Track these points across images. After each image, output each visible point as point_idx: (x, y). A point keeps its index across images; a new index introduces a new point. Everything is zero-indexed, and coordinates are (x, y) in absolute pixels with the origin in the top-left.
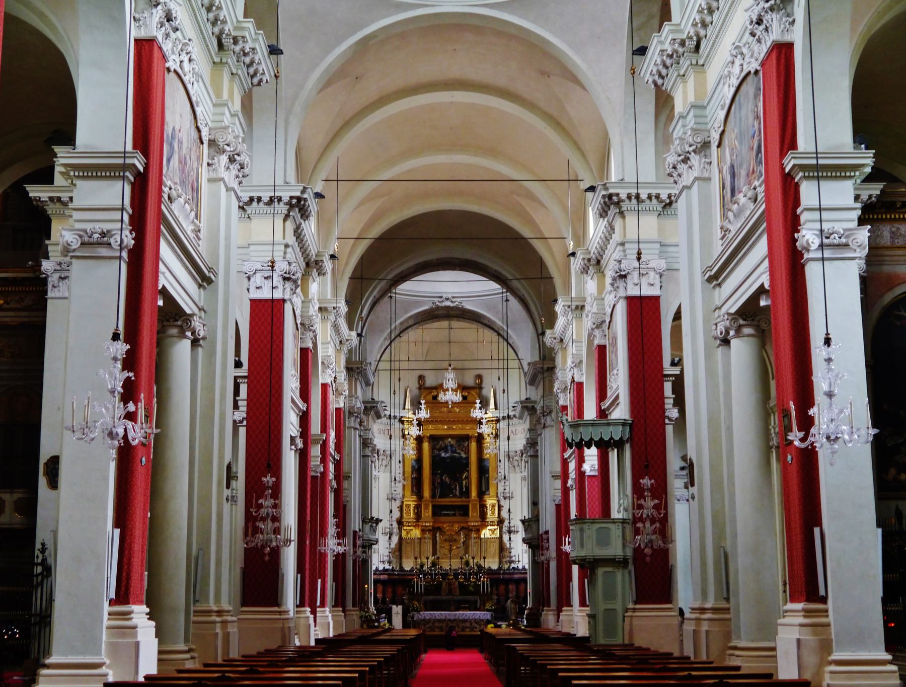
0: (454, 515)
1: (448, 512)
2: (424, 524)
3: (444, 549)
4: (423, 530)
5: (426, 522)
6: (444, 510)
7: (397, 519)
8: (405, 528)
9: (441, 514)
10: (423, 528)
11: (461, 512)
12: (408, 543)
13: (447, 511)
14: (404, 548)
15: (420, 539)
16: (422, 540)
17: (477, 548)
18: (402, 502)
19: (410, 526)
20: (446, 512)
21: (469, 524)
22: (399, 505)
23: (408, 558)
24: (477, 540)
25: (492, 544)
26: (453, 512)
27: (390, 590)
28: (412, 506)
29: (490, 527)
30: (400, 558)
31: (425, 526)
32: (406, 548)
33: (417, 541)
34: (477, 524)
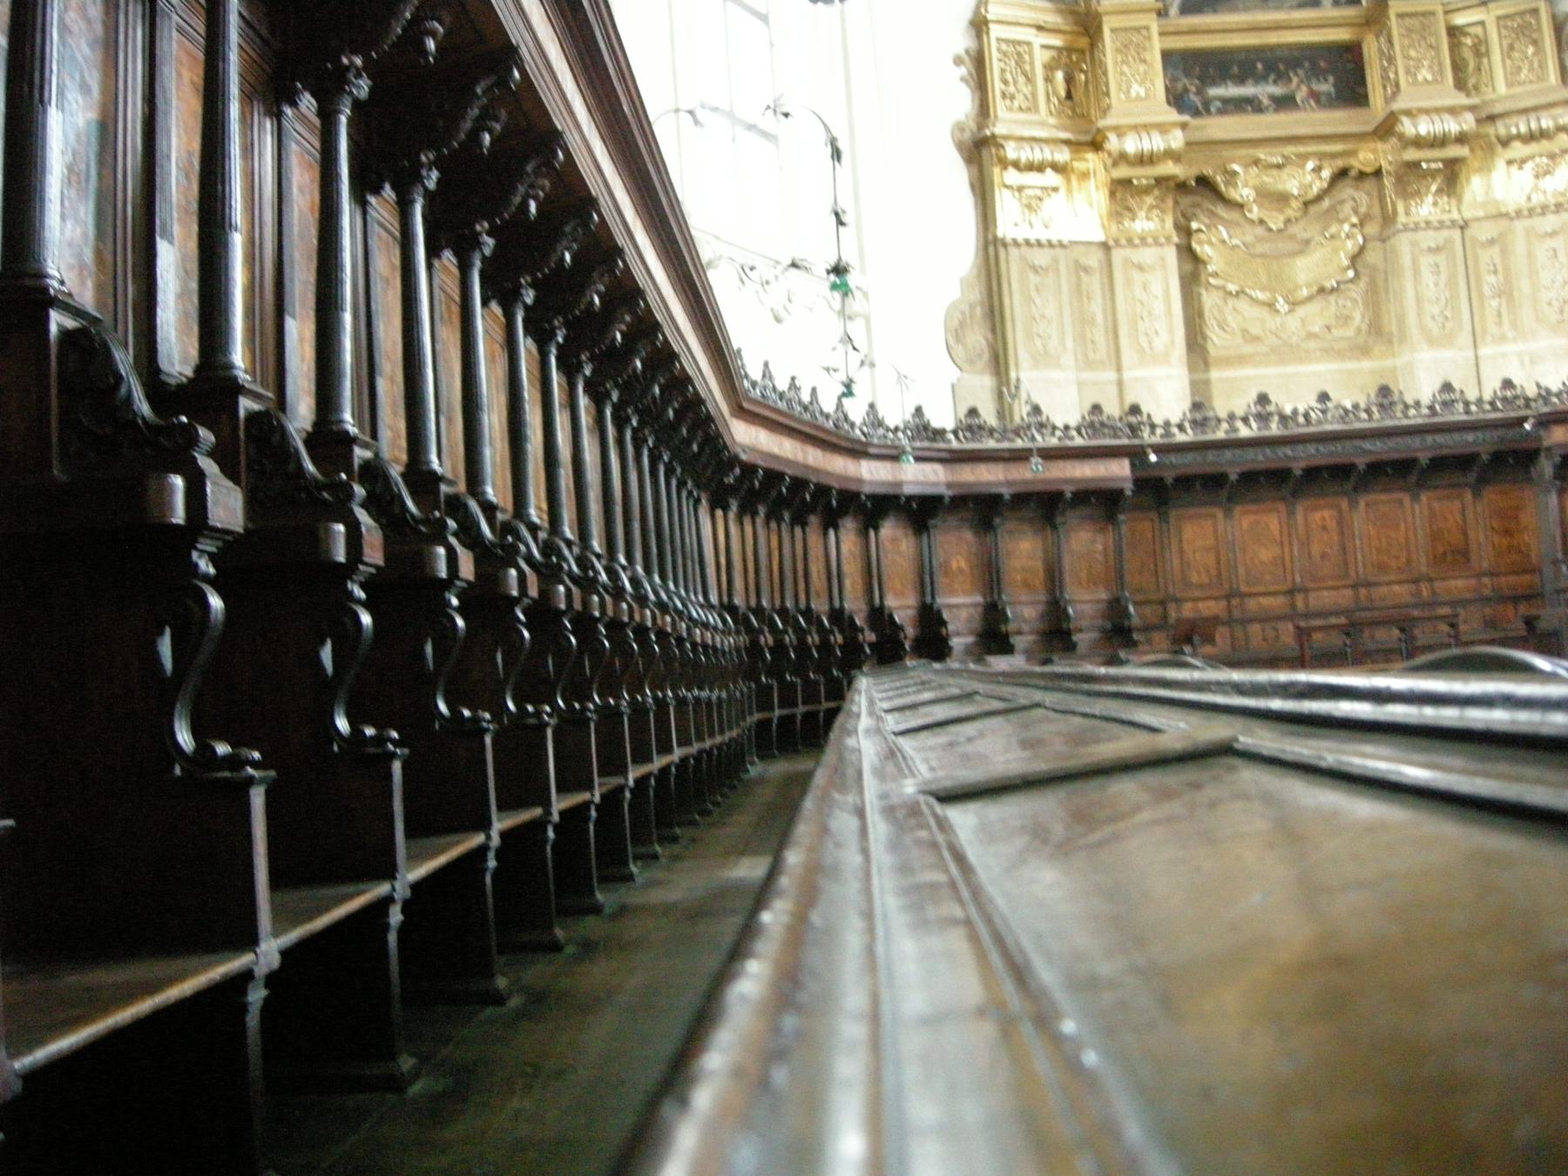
0: (1285, 103)
1: (1248, 90)
2: (1131, 145)
3: (1243, 304)
4: (1121, 189)
5: (1147, 127)
6: (1223, 75)
7: (959, 127)
8: (1012, 176)
9: (1207, 104)
10: (1123, 172)
11: (1326, 87)
12: (1035, 269)
13: (1241, 80)
14: (1015, 304)
15: (1105, 247)
16: (1118, 255)
17: (1452, 283)
18: (979, 25)
19: (1039, 168)
20: (1233, 91)
21: (1407, 127)
22: (961, 52)
23: (1044, 359)
24: (1445, 233)
25: (1541, 251)
26: (1277, 90)
27: (960, 563)
28: (1041, 57)
29: (1518, 151)
30: (998, 362)
31: (1144, 160)
32: (1029, 300)
33: (1094, 259)
34: (1452, 126)
